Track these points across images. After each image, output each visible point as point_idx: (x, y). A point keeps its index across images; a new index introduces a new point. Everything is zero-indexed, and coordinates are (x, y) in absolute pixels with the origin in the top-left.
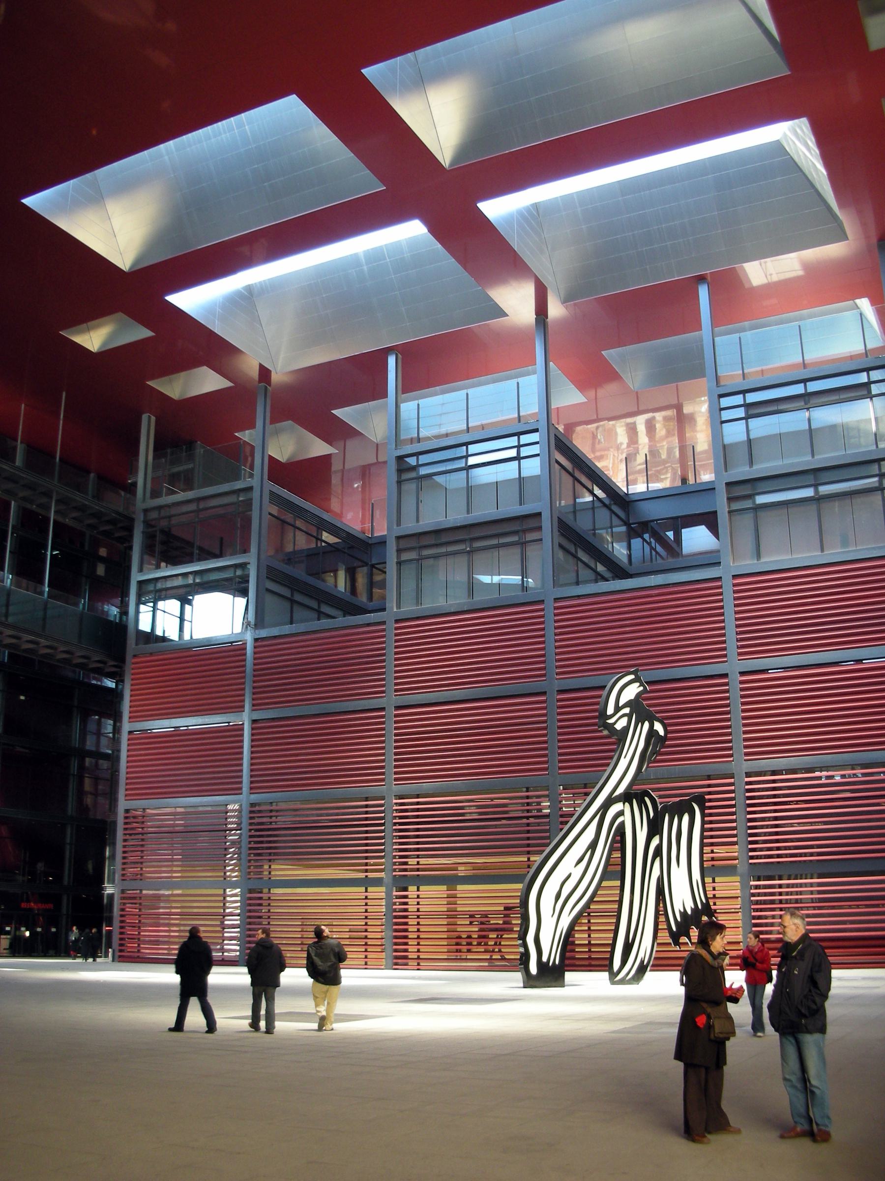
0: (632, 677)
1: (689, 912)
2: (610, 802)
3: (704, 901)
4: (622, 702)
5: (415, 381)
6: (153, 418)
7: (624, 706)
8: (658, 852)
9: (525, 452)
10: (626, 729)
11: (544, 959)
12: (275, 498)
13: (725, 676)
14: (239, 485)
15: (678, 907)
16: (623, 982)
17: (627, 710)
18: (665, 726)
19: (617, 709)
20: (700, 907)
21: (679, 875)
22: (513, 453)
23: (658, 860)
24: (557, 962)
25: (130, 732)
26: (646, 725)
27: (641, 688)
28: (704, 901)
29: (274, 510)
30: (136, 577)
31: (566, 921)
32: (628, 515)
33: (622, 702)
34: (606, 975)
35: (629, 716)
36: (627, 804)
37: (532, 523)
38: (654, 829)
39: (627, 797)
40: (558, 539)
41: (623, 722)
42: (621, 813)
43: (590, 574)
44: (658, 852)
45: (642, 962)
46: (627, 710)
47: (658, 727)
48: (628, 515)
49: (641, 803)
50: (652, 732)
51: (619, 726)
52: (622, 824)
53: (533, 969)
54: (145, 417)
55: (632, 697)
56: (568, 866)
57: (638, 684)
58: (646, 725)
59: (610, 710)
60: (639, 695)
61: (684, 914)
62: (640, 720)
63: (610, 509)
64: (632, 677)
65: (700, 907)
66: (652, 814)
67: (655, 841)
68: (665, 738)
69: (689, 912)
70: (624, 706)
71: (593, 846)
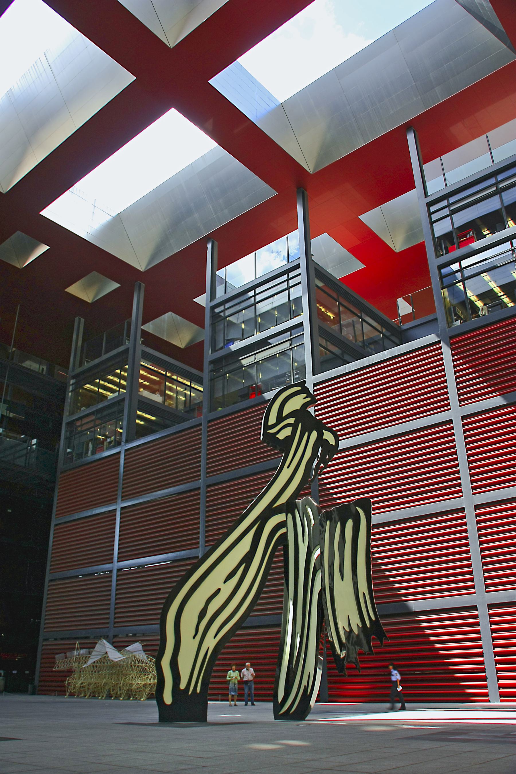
0: (299, 388)
1: (356, 630)
2: (270, 511)
3: (373, 618)
5: (225, 259)
6: (82, 320)
7: (289, 416)
9: (292, 282)
10: (289, 439)
11: (183, 686)
14: (121, 349)
15: (342, 624)
16: (287, 716)
17: (292, 420)
18: (334, 433)
19: (280, 418)
20: (368, 625)
21: (343, 589)
22: (285, 286)
24: (198, 690)
25: (56, 525)
26: (314, 435)
27: (309, 399)
28: (373, 618)
31: (211, 642)
34: (270, 705)
35: (295, 426)
36: (289, 515)
41: (287, 432)
42: (283, 524)
45: (305, 690)
46: (292, 420)
47: (328, 436)
50: (320, 441)
51: (281, 436)
52: (285, 535)
53: (168, 698)
54: (77, 319)
56: (215, 580)
57: (305, 395)
58: (314, 435)
59: (272, 420)
60: (305, 406)
61: (349, 633)
62: (307, 429)
63: (363, 320)
64: (299, 388)
65: (368, 625)
67: (317, 553)
69: (356, 630)
70: (289, 416)
71: (248, 559)
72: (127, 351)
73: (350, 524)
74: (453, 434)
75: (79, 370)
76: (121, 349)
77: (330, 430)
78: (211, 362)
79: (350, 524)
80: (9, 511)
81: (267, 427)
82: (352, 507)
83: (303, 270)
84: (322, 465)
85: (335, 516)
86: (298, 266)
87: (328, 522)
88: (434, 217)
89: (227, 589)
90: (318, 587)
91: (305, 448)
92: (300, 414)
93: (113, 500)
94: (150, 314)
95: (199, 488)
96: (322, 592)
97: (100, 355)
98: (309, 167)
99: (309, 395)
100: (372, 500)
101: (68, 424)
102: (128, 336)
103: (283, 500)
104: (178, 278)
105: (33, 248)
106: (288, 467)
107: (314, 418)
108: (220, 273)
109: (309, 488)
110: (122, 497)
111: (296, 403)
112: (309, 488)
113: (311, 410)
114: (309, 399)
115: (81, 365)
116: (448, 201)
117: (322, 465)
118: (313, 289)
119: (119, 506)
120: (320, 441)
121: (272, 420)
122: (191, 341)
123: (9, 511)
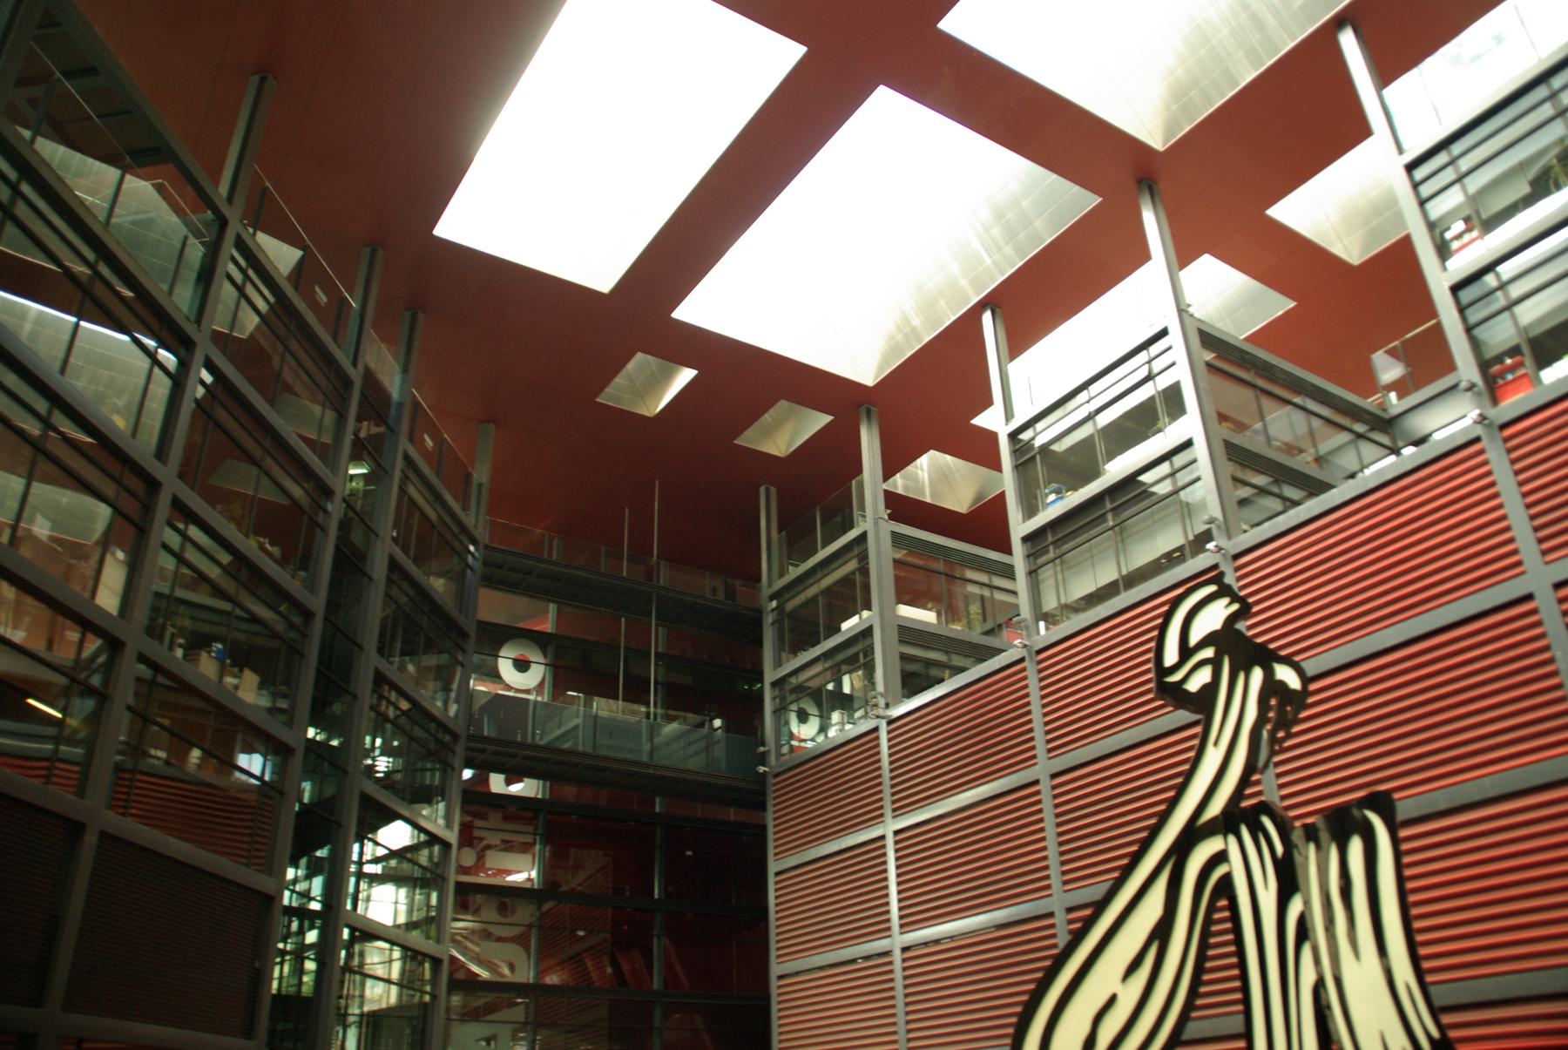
0: (1212, 588)
2: (1192, 835)
4: (1194, 639)
6: (773, 490)
7: (1202, 644)
8: (1303, 932)
10: (1210, 690)
12: (897, 539)
13: (1529, 597)
14: (853, 534)
17: (1209, 653)
19: (1186, 652)
23: (1307, 952)
25: (777, 874)
26: (1257, 675)
29: (900, 555)
30: (770, 675)
32: (1394, 440)
33: (1194, 639)
35: (1216, 663)
36: (1232, 839)
37: (1179, 460)
38: (1288, 884)
39: (1228, 823)
40: (1229, 468)
41: (1203, 677)
42: (1220, 857)
43: (1274, 504)
44: (1303, 932)
46: (1209, 653)
47: (1285, 674)
48: (1394, 440)
49: (1257, 830)
50: (1272, 687)
51: (1193, 685)
52: (1227, 880)
54: (762, 490)
55: (1217, 625)
56: (1106, 978)
57: (1226, 600)
58: (1257, 675)
59: (1171, 656)
60: (1231, 620)
62: (1242, 666)
64: (1212, 588)
66: (1279, 849)
67: (1295, 907)
68: (1305, 692)
71: (1161, 932)
72: (863, 538)
73: (1356, 847)
74: (1547, 648)
75: (780, 584)
76: (853, 534)
77: (1287, 661)
78: (1025, 539)
79: (1356, 847)
80: (689, 853)
81: (1163, 672)
82: (1355, 812)
83: (1175, 338)
84: (1281, 734)
85: (1324, 836)
86: (1163, 333)
87: (1312, 848)
88: (1426, 190)
89: (1129, 995)
90: (1308, 977)
91: (1243, 701)
92: (1224, 639)
93: (879, 818)
94: (894, 462)
95: (1036, 782)
96: (1319, 987)
97: (815, 552)
98: (1158, 143)
99: (1235, 598)
100: (1396, 796)
101: (774, 684)
102: (862, 507)
103: (1215, 808)
104: (936, 389)
105: (667, 377)
106: (1216, 744)
107: (1249, 640)
108: (1013, 368)
109: (1258, 782)
110: (894, 810)
111: (1214, 617)
112: (1258, 782)
113: (1241, 626)
114: (1235, 607)
115: (782, 575)
116: (1457, 170)
117: (1281, 734)
118: (1202, 369)
119: (890, 826)
120: (1272, 687)
121: (1171, 656)
122: (978, 498)
123: (689, 853)
